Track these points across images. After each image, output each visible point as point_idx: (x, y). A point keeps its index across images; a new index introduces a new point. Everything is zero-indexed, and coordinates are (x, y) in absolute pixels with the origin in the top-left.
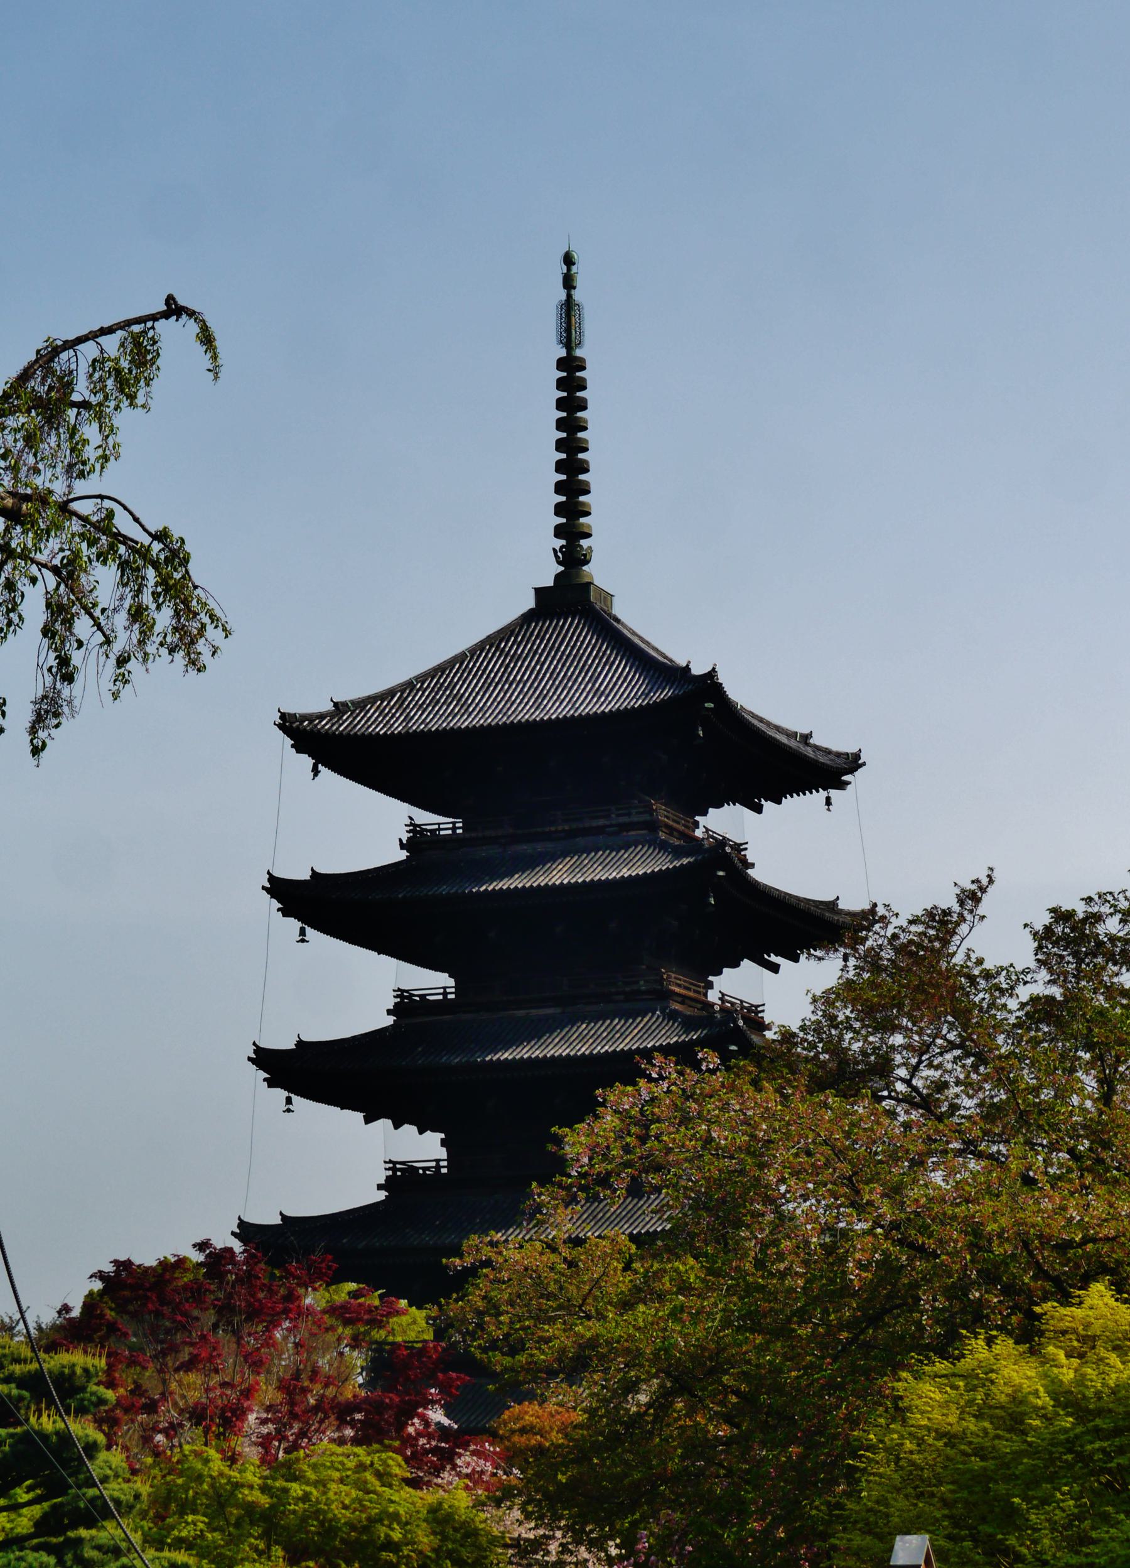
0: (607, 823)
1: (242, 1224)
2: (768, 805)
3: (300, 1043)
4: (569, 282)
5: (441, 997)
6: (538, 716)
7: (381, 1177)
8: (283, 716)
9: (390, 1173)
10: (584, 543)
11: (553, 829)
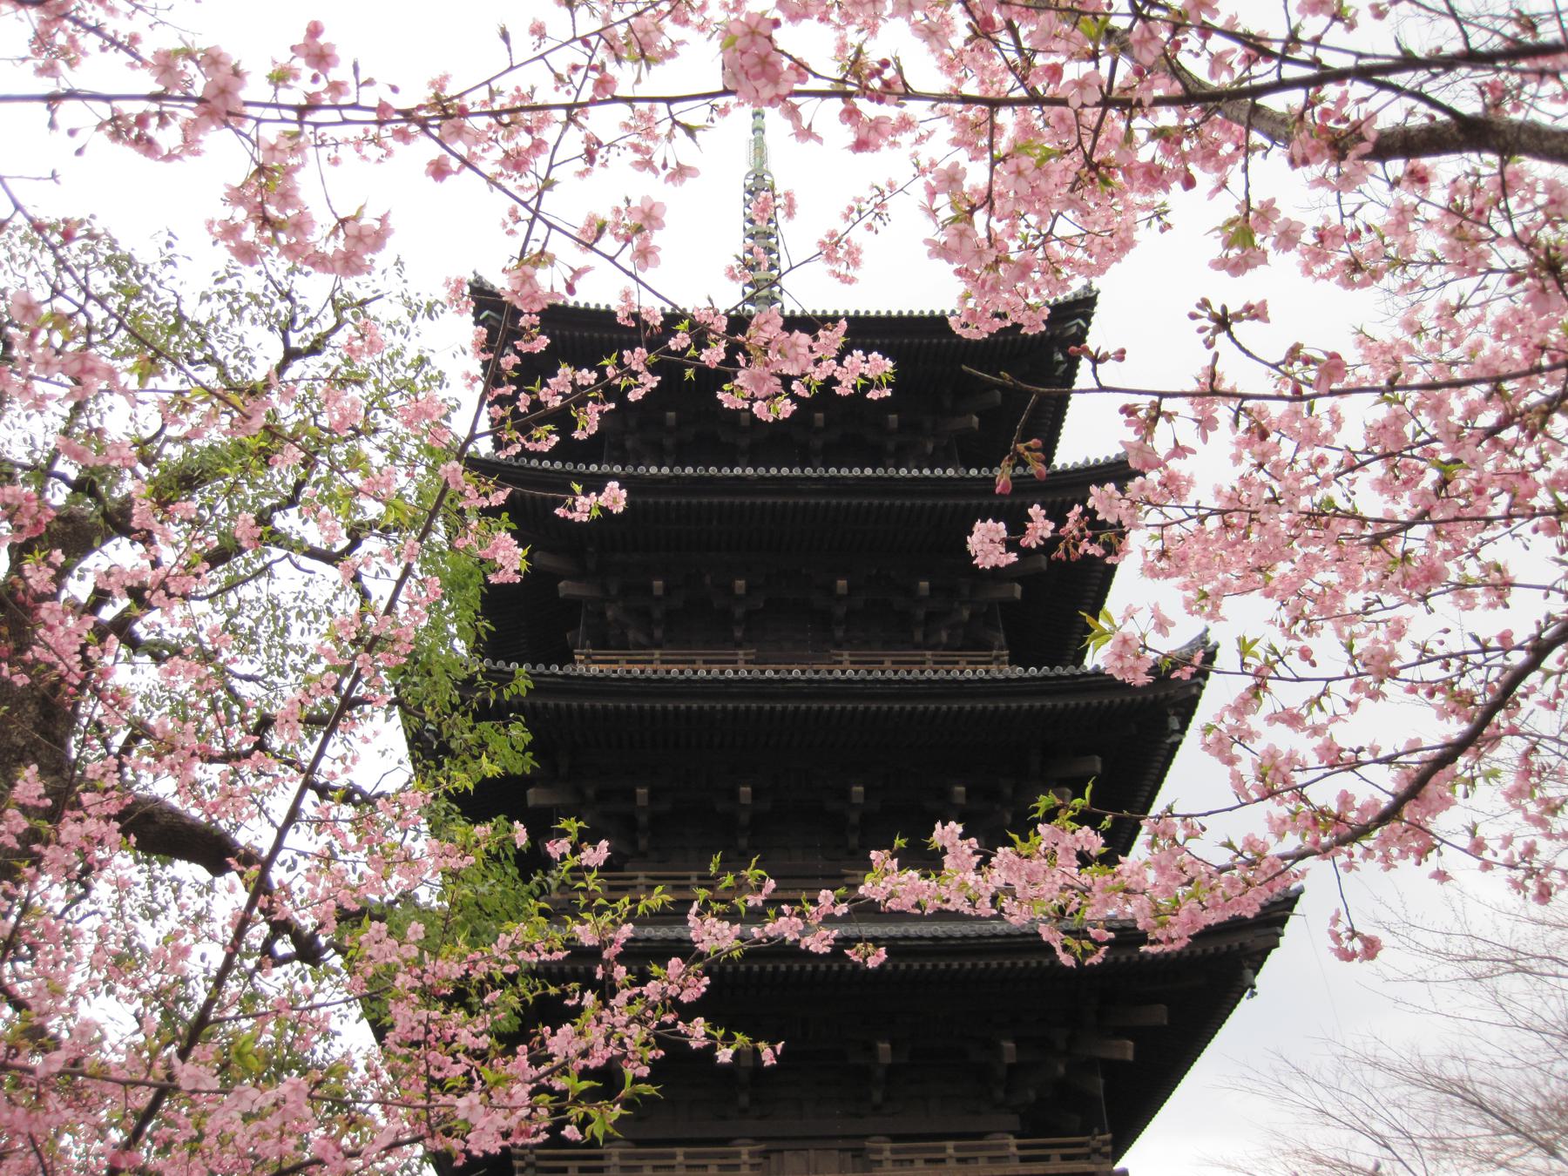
8: (479, 279)
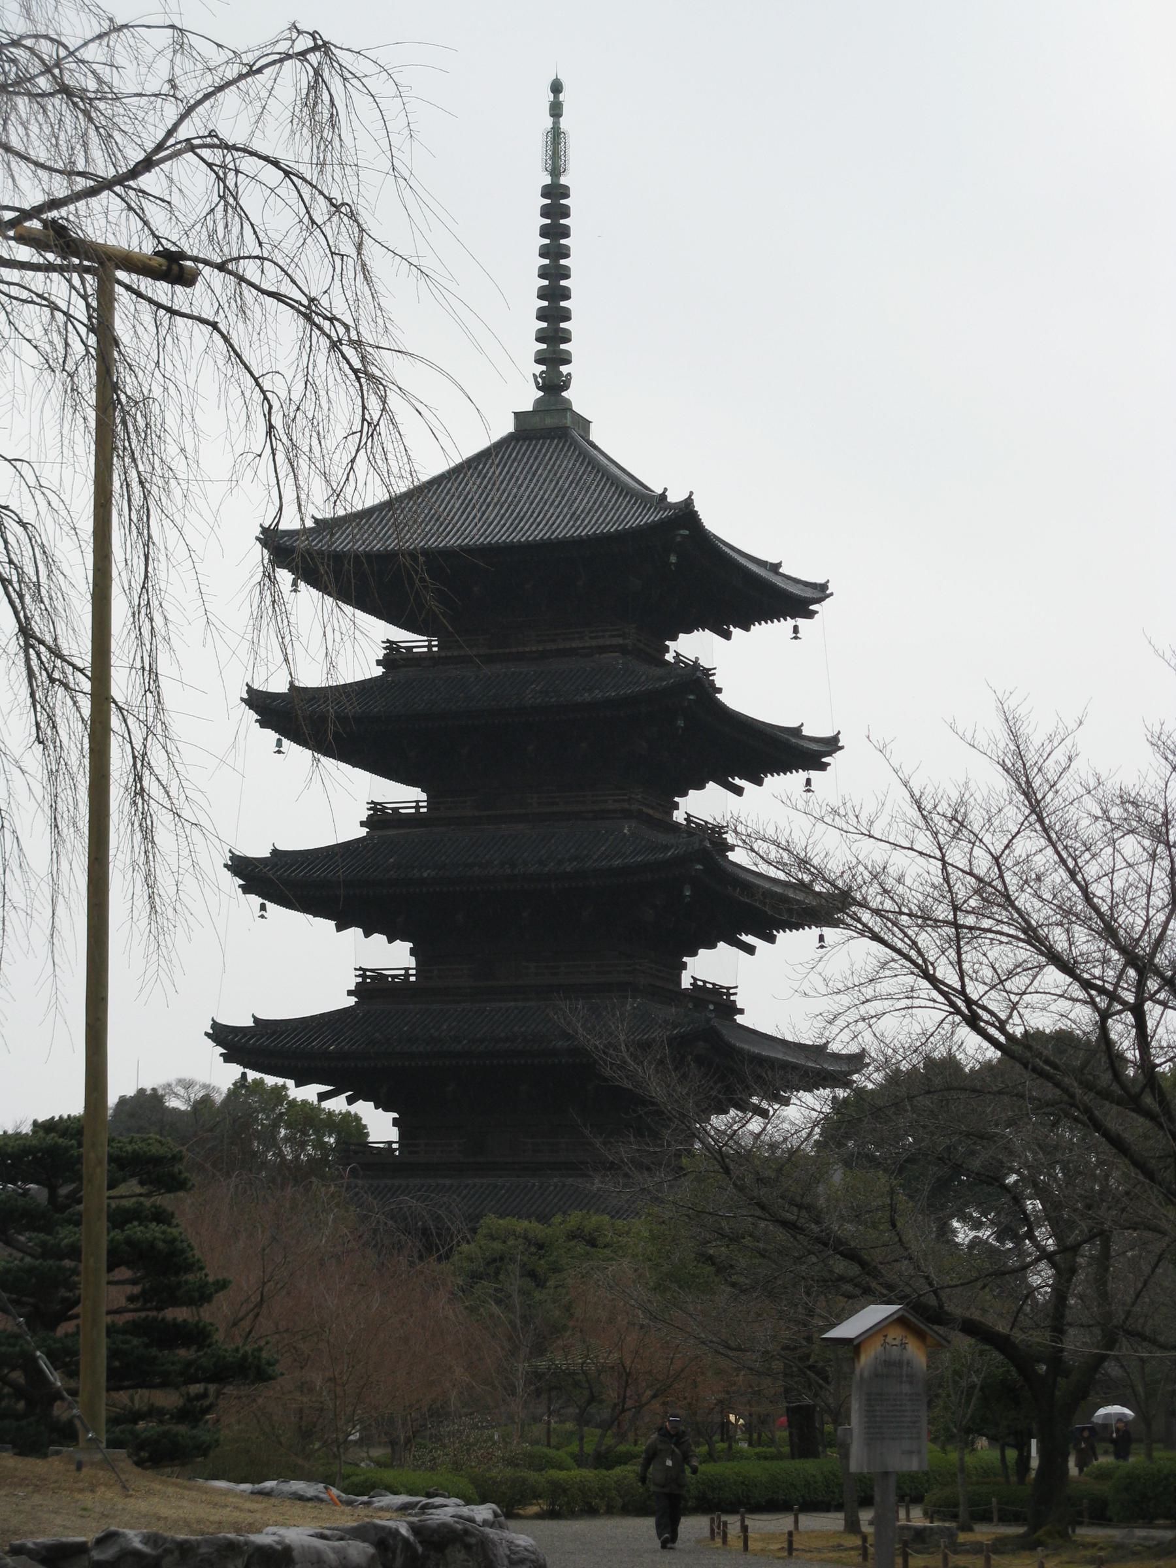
0: (581, 645)
1: (215, 1025)
2: (736, 632)
3: (275, 852)
4: (556, 110)
5: (413, 811)
6: (516, 537)
7: (352, 983)
9: (360, 980)
10: (564, 369)
11: (527, 649)
